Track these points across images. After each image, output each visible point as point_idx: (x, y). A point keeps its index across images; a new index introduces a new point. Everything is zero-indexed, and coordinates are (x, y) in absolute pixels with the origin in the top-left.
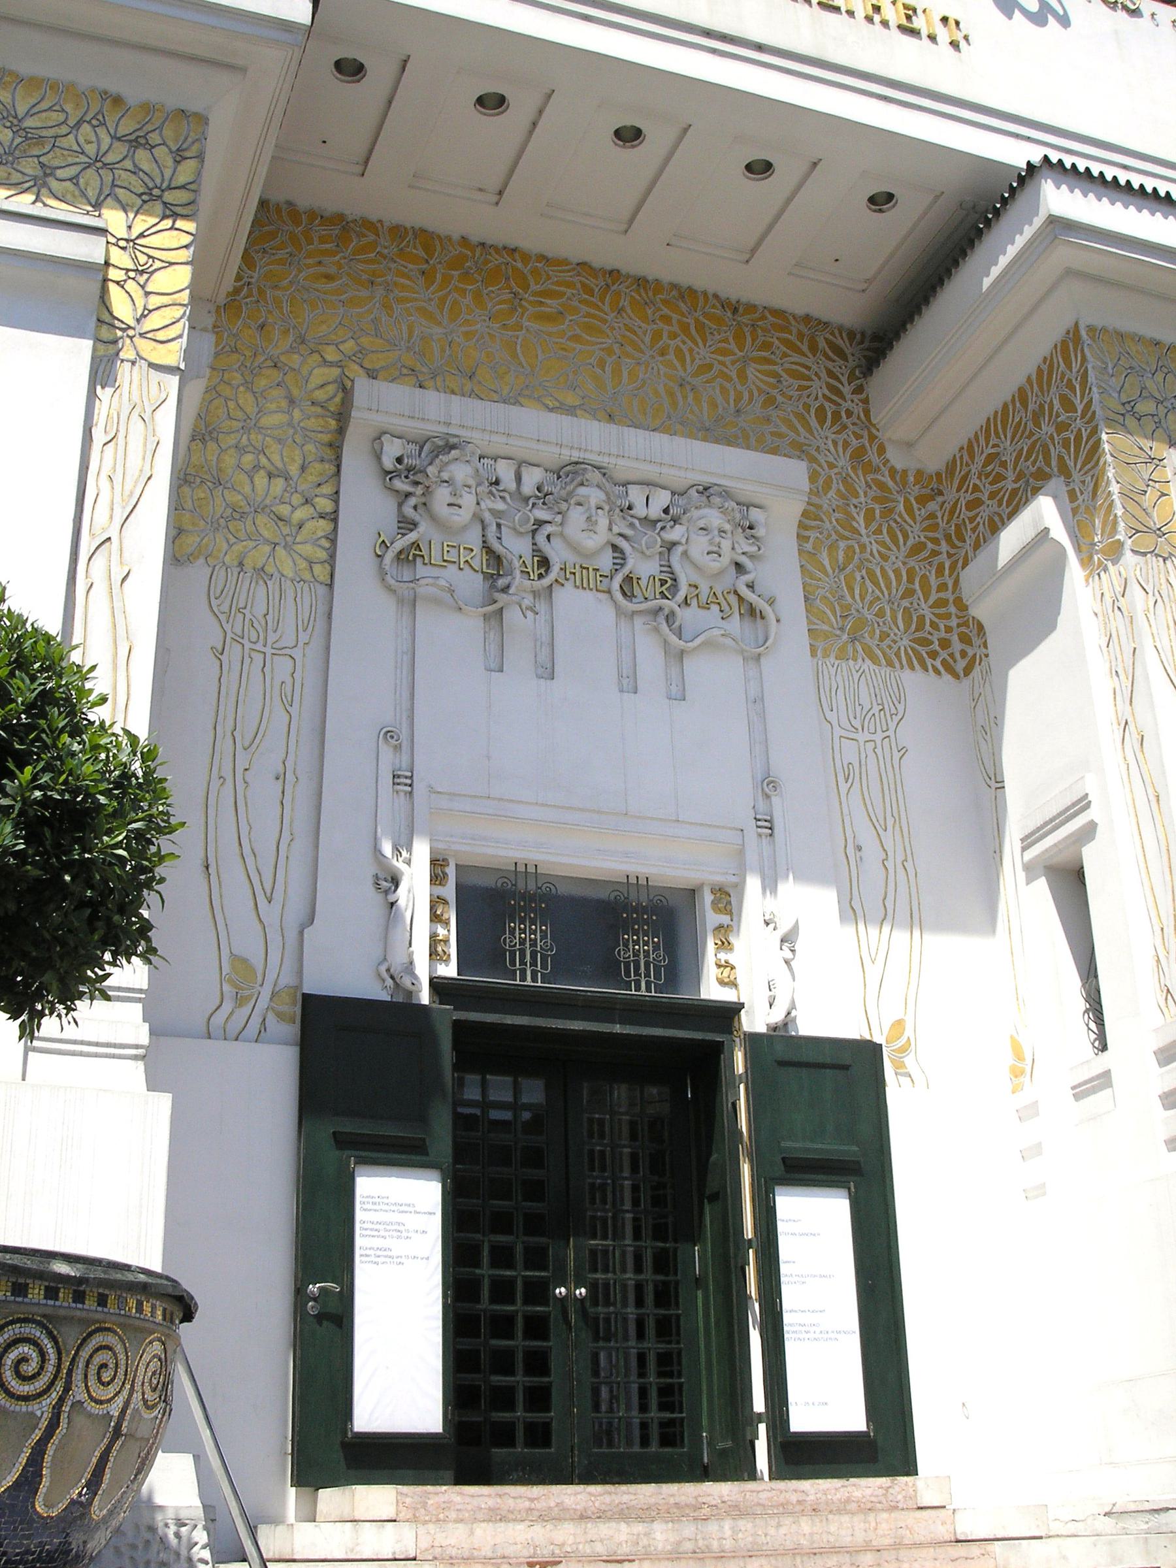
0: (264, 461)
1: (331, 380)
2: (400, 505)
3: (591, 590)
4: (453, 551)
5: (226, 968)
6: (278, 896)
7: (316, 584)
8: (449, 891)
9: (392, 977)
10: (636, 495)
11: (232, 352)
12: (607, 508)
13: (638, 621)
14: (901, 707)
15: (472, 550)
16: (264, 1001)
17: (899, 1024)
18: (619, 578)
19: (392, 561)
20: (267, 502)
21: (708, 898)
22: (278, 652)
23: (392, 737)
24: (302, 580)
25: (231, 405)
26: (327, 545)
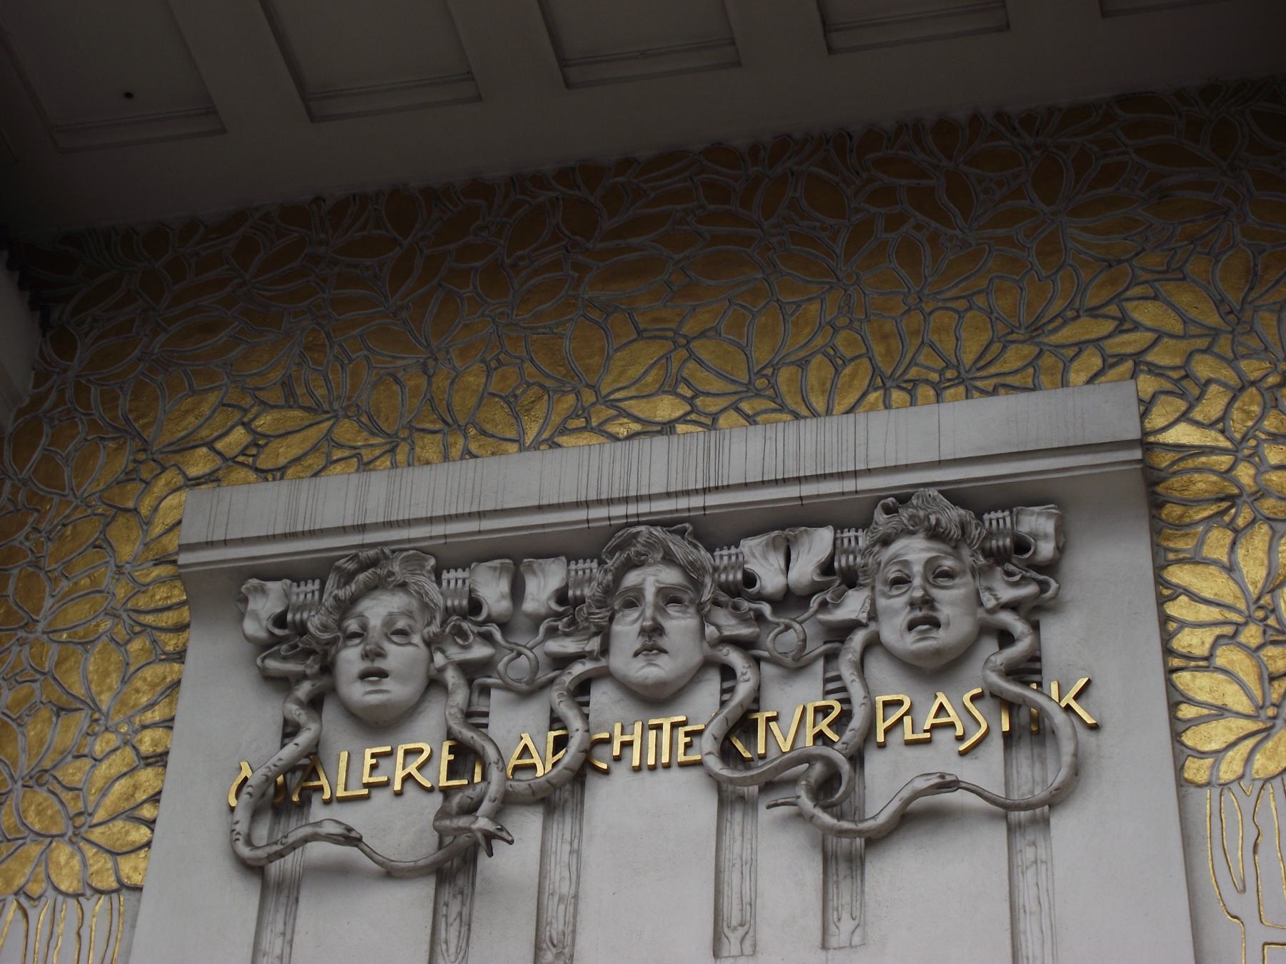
3: (667, 766)
7: (124, 891)
15: (421, 751)
18: (716, 728)
20: (47, 764)
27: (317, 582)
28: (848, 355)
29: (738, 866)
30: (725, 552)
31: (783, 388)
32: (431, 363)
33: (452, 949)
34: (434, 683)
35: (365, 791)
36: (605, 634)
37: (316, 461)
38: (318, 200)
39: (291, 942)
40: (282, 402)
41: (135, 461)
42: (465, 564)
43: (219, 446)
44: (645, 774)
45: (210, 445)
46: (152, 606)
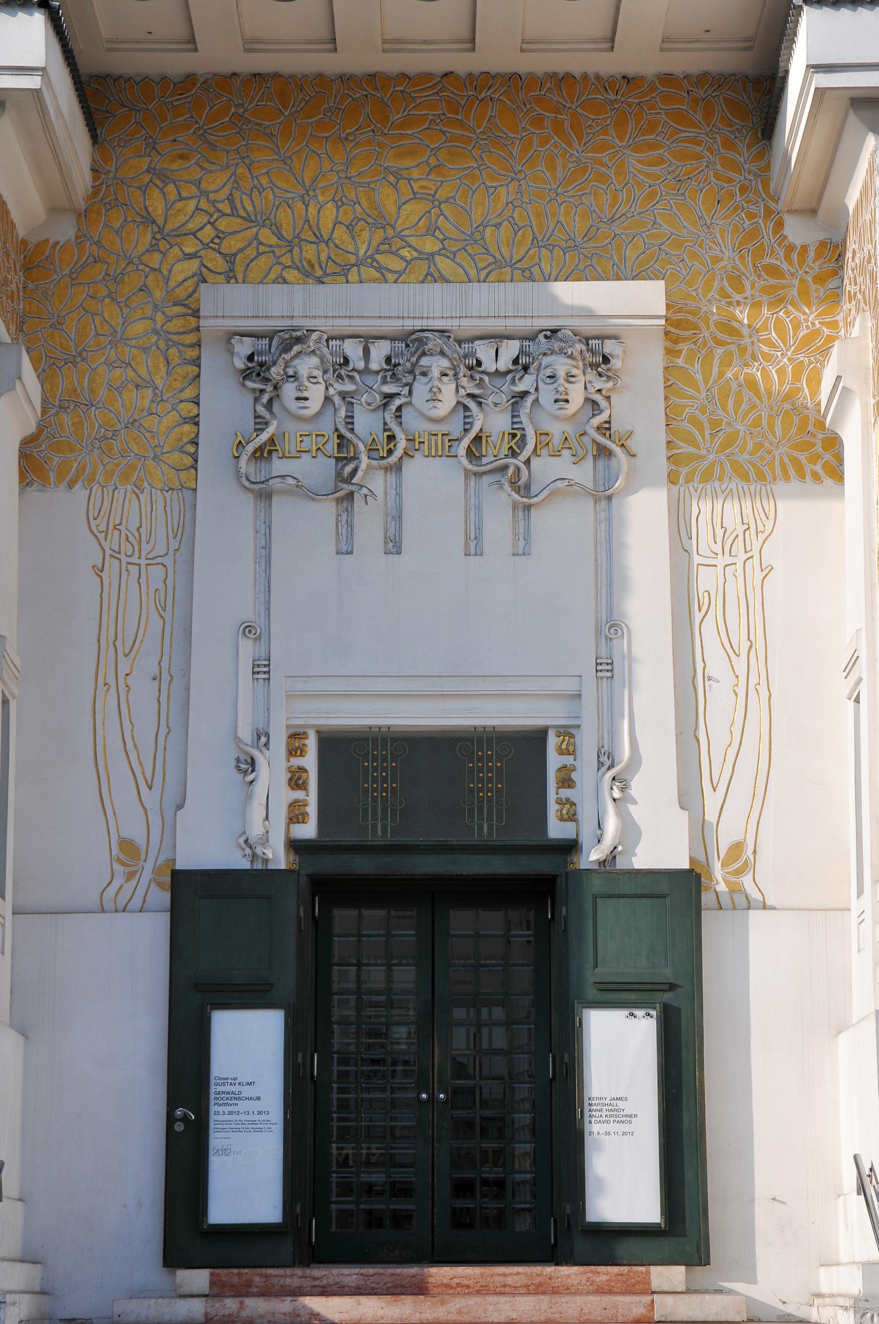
0: (131, 374)
1: (190, 274)
2: (256, 400)
3: (441, 456)
4: (304, 438)
5: (115, 851)
6: (157, 782)
7: (183, 489)
8: (310, 761)
9: (251, 847)
10: (484, 352)
11: (96, 262)
12: (451, 373)
13: (487, 480)
14: (769, 524)
15: (324, 435)
16: (147, 874)
17: (737, 848)
19: (249, 460)
21: (552, 741)
22: (152, 561)
23: (250, 631)
24: (171, 489)
25: (97, 318)
26: (192, 450)
27: (267, 339)
28: (521, 225)
29: (473, 509)
30: (466, 346)
31: (488, 240)
32: (306, 197)
33: (345, 539)
34: (328, 399)
35: (299, 455)
36: (410, 385)
37: (251, 252)
38: (234, 74)
39: (270, 527)
40: (229, 211)
41: (154, 238)
42: (342, 338)
43: (200, 235)
44: (431, 459)
45: (194, 234)
46: (177, 330)
